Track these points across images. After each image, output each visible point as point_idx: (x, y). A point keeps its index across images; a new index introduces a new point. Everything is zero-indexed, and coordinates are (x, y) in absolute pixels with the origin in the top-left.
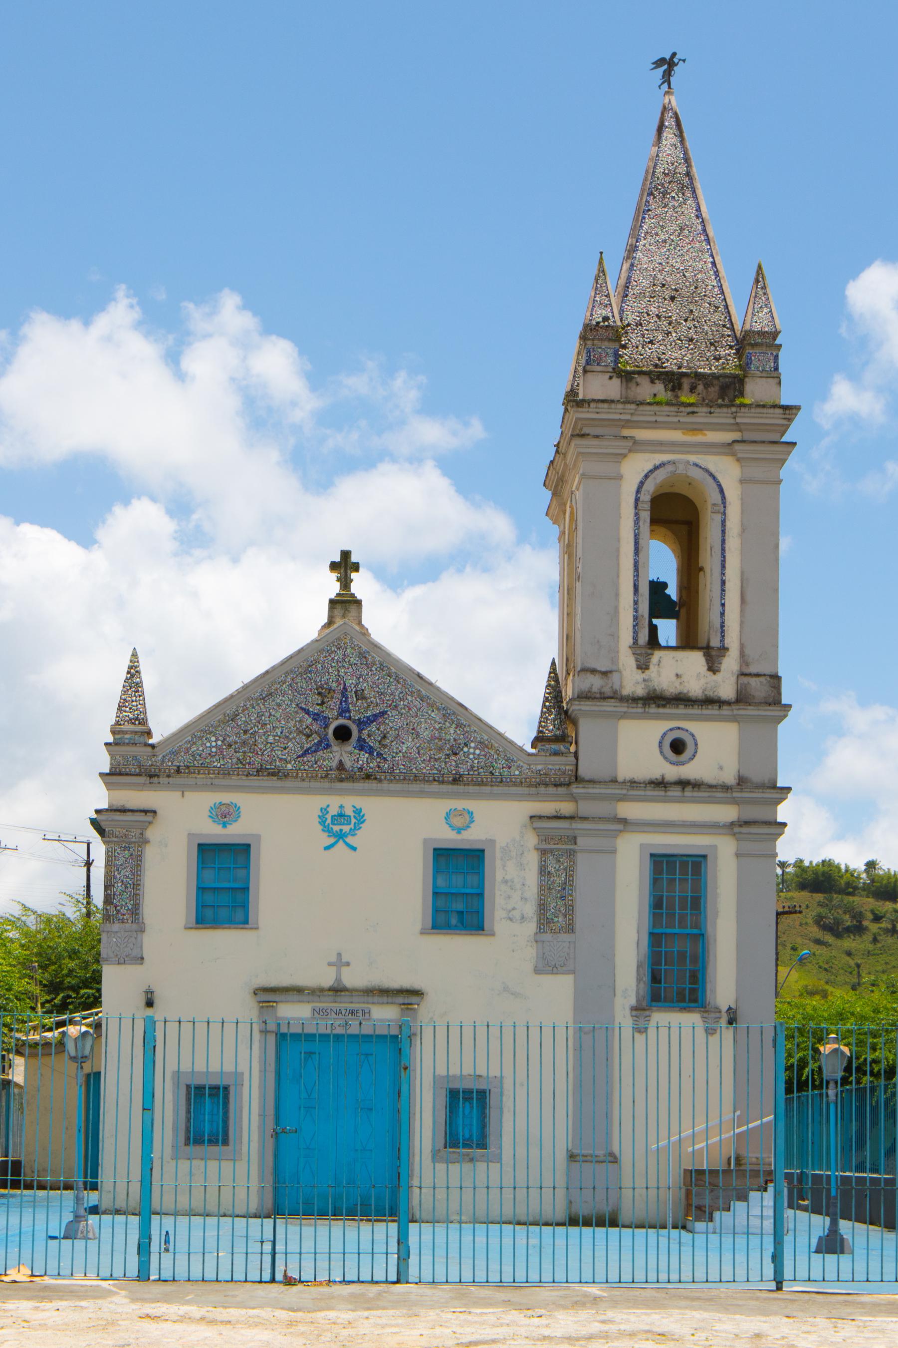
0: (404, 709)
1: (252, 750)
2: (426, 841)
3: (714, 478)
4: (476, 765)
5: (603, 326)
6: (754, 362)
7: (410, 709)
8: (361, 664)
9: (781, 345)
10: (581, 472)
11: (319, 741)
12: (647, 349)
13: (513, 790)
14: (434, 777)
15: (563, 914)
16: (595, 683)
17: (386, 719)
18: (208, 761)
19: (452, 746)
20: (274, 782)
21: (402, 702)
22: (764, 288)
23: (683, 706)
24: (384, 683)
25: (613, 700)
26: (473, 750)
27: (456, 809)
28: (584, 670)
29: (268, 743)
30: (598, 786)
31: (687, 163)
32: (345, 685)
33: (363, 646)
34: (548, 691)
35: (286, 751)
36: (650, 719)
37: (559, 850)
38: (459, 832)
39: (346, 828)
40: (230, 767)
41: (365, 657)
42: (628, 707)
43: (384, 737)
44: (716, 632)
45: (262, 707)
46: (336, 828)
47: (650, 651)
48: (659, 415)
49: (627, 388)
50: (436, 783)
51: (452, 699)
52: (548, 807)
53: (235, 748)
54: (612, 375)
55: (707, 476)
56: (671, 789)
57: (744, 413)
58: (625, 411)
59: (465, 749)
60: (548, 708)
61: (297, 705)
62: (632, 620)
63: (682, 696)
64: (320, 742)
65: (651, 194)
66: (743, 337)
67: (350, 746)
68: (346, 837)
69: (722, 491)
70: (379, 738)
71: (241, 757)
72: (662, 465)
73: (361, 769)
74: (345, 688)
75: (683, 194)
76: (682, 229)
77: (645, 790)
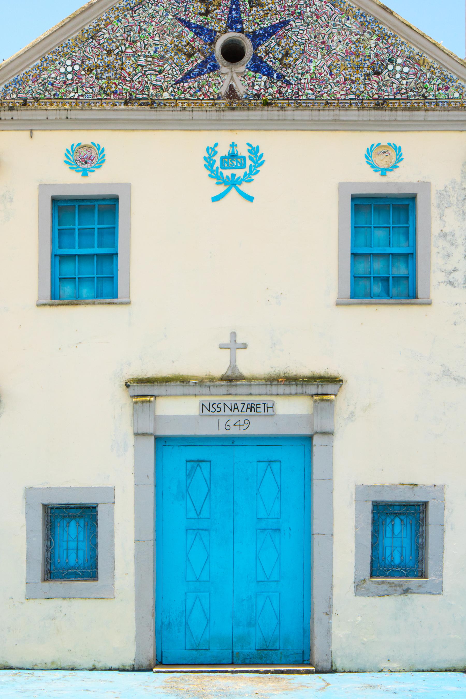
0: (311, 17)
1: (118, 76)
2: (341, 186)
7: (318, 17)
11: (203, 62)
18: (62, 91)
19: (373, 63)
27: (379, 145)
39: (240, 173)
43: (287, 54)
45: (130, 19)
53: (97, 74)
59: (390, 67)
61: (175, 16)
64: (204, 63)
67: (241, 68)
70: (280, 56)
71: (103, 82)
73: (257, 96)
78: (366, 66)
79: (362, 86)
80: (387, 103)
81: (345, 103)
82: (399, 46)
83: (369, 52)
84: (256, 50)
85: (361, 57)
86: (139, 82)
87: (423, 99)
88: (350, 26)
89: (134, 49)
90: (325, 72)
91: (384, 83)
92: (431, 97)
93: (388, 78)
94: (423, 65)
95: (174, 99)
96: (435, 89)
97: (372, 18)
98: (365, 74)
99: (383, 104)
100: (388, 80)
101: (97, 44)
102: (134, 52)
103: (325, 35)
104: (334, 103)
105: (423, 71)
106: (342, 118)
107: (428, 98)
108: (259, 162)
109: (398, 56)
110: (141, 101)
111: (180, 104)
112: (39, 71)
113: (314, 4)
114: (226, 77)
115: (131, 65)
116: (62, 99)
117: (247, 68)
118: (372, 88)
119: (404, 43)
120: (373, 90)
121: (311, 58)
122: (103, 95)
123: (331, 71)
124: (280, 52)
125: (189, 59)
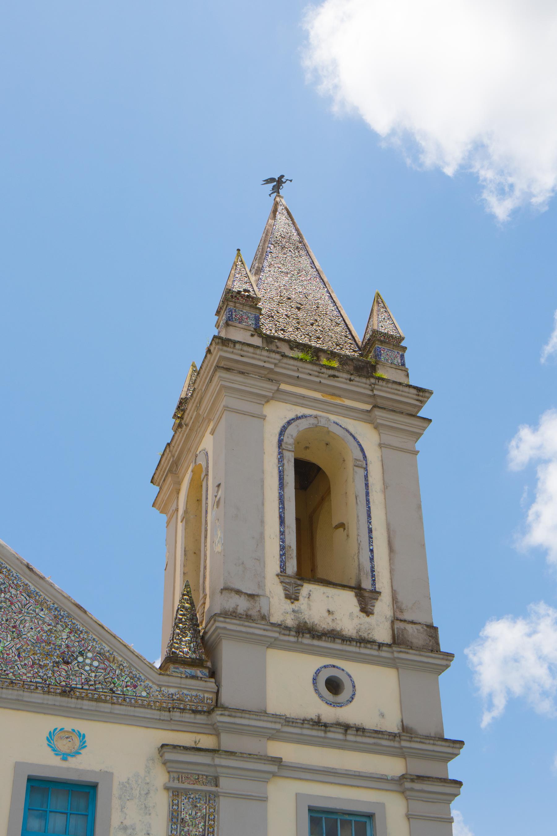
0: (5, 602)
2: (18, 766)
3: (354, 438)
4: (92, 679)
5: (244, 295)
6: (383, 355)
7: (12, 604)
9: (406, 348)
10: (224, 403)
13: (140, 712)
19: (64, 652)
22: (384, 307)
27: (62, 730)
30: (247, 716)
34: (181, 612)
36: (302, 652)
37: (196, 791)
38: (64, 759)
42: (280, 633)
44: (367, 575)
47: (299, 582)
48: (301, 372)
51: (68, 598)
56: (332, 729)
57: (382, 386)
58: (270, 360)
59: (80, 659)
60: (183, 631)
62: (278, 548)
66: (364, 346)
69: (362, 450)
72: (304, 417)
77: (301, 728)
78: (56, 654)
79: (50, 672)
80: (74, 691)
81: (31, 685)
82: (91, 642)
83: (60, 642)
85: (52, 645)
87: (110, 693)
88: (44, 616)
90: (13, 653)
91: (73, 672)
92: (119, 692)
93: (77, 668)
94: (113, 662)
96: (123, 685)
97: (65, 613)
98: (54, 662)
99: (70, 692)
100: (76, 671)
103: (17, 620)
104: (20, 683)
105: (112, 667)
106: (25, 699)
107: (116, 692)
109: (89, 650)
113: (9, 592)
118: (60, 675)
119: (96, 640)
120: (61, 677)
123: (19, 653)
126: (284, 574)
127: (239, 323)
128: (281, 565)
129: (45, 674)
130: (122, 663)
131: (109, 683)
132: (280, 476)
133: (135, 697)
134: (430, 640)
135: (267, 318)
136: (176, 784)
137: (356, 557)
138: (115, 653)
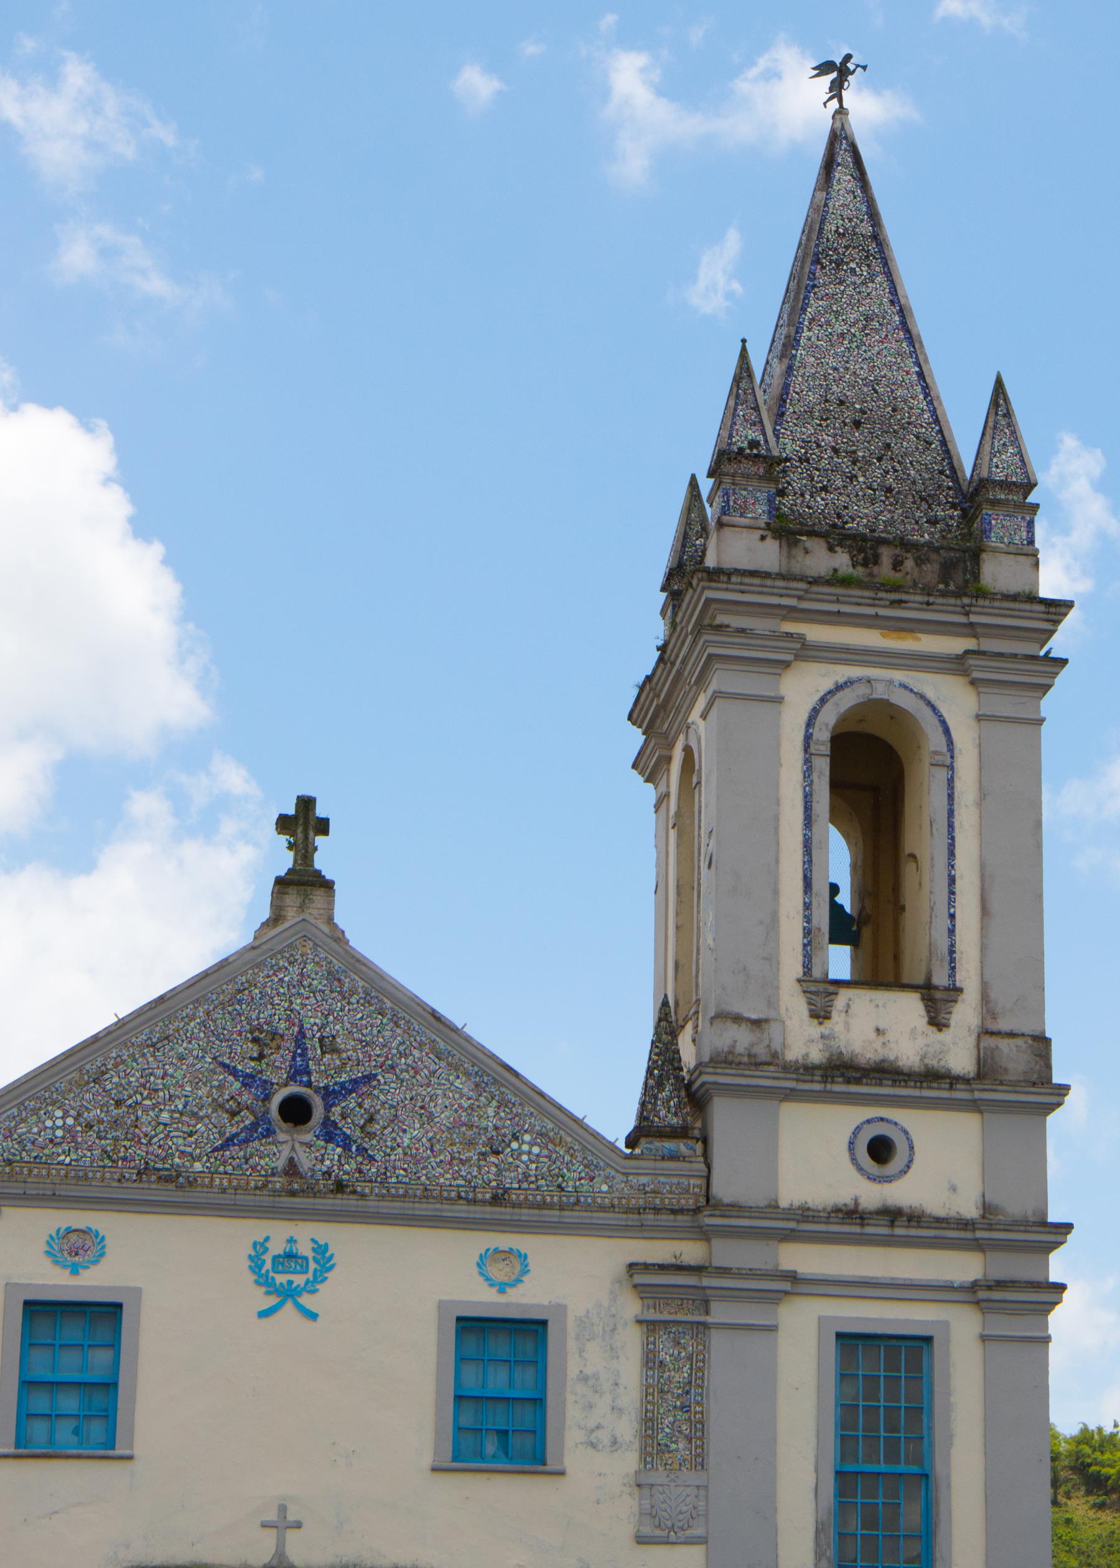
0: (407, 1071)
1: (129, 1136)
2: (442, 1306)
3: (934, 709)
5: (749, 455)
6: (995, 529)
7: (416, 1073)
8: (332, 992)
12: (819, 499)
14: (459, 1193)
15: (686, 1436)
16: (741, 1038)
17: (375, 1088)
18: (46, 1151)
20: (168, 1193)
21: (403, 1060)
23: (890, 1083)
24: (372, 1026)
25: (772, 1068)
26: (527, 1145)
28: (722, 1016)
29: (159, 1124)
31: (873, 220)
32: (301, 1027)
33: (335, 961)
34: (657, 1050)
35: (192, 1139)
38: (502, 1292)
39: (299, 1280)
40: (88, 1164)
41: (339, 980)
43: (371, 1120)
44: (942, 960)
45: (151, 1059)
46: (281, 1279)
49: (790, 556)
50: (461, 1202)
51: (493, 1057)
52: (659, 1251)
53: (99, 1132)
54: (765, 533)
55: (922, 704)
56: (872, 1222)
59: (515, 1145)
61: (215, 1058)
62: (800, 934)
63: (886, 1065)
64: (254, 1126)
65: (817, 261)
68: (300, 1295)
69: (947, 731)
70: (362, 1122)
72: (849, 683)
73: (328, 1174)
74: (302, 1033)
75: (869, 266)
76: (868, 319)
79: (475, 1169)
84: (329, 1112)
86: (160, 1147)
88: (461, 1086)
89: (154, 1101)
93: (511, 1160)
95: (209, 1172)
98: (479, 1153)
101: (101, 1091)
102: (153, 1104)
108: (328, 1265)
110: (162, 1173)
111: (218, 1180)
112: (14, 1123)
114: (284, 1146)
115: (150, 1123)
116: (46, 1163)
117: (316, 1136)
118: (488, 1172)
121: (404, 1127)
122: (106, 1161)
123: (432, 1146)
124: (362, 1115)
125: (233, 1119)
126: (809, 979)
127: (741, 516)
128: (804, 962)
129: (469, 1173)
130: (572, 1145)
131: (556, 1178)
132: (806, 803)
133: (592, 1194)
134: (1037, 1062)
135: (797, 467)
136: (652, 1315)
137: (927, 928)
138: (562, 1132)
